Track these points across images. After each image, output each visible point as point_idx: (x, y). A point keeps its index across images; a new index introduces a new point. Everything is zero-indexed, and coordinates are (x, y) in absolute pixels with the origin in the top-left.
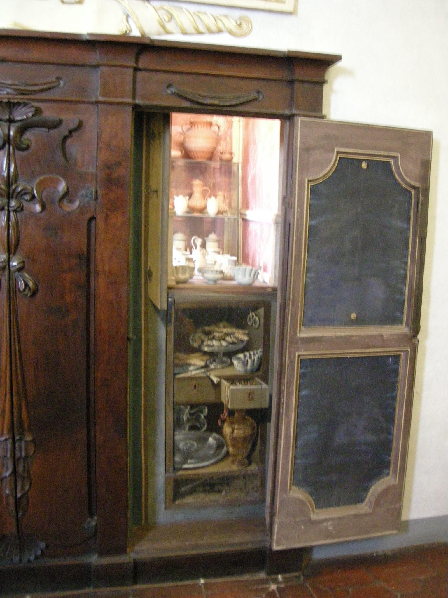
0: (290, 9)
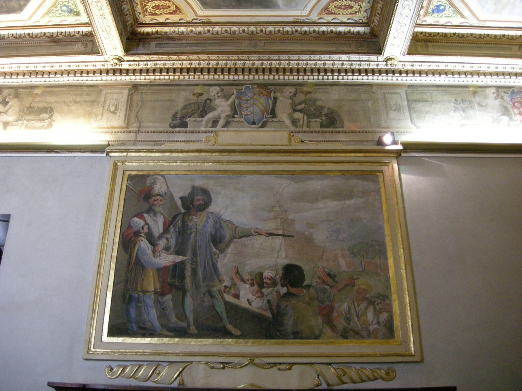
0: (419, 360)
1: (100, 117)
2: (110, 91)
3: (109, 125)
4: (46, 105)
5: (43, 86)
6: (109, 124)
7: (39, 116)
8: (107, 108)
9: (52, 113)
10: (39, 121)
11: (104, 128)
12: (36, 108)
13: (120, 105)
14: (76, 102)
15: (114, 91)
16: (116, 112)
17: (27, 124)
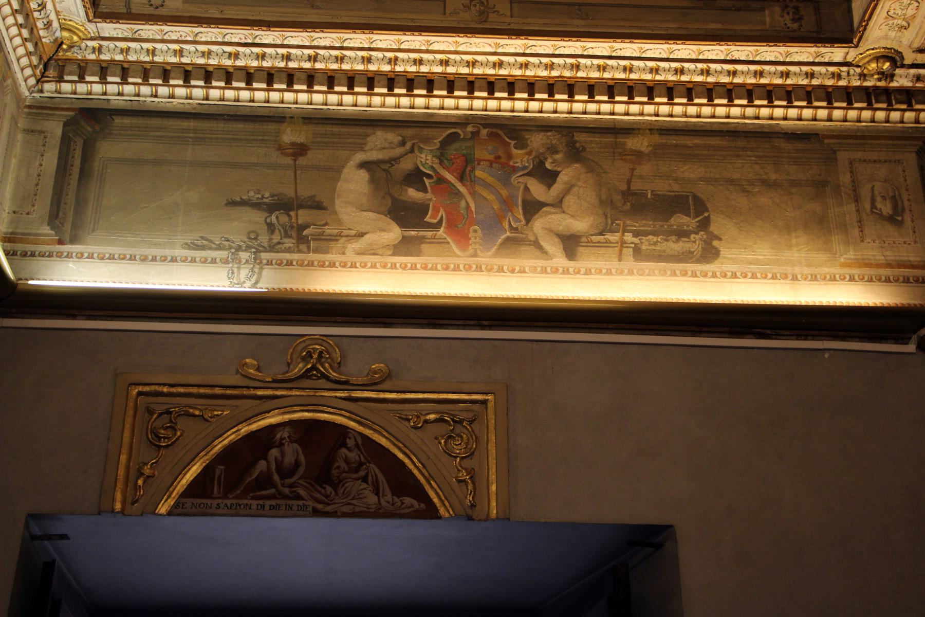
1: (856, 232)
2: (859, 155)
3: (893, 258)
4: (676, 187)
5: (650, 130)
6: (891, 256)
7: (667, 220)
8: (868, 206)
9: (706, 214)
10: (674, 238)
11: (879, 266)
12: (649, 196)
13: (905, 197)
14: (769, 185)
15: (875, 156)
16: (900, 218)
17: (636, 244)
